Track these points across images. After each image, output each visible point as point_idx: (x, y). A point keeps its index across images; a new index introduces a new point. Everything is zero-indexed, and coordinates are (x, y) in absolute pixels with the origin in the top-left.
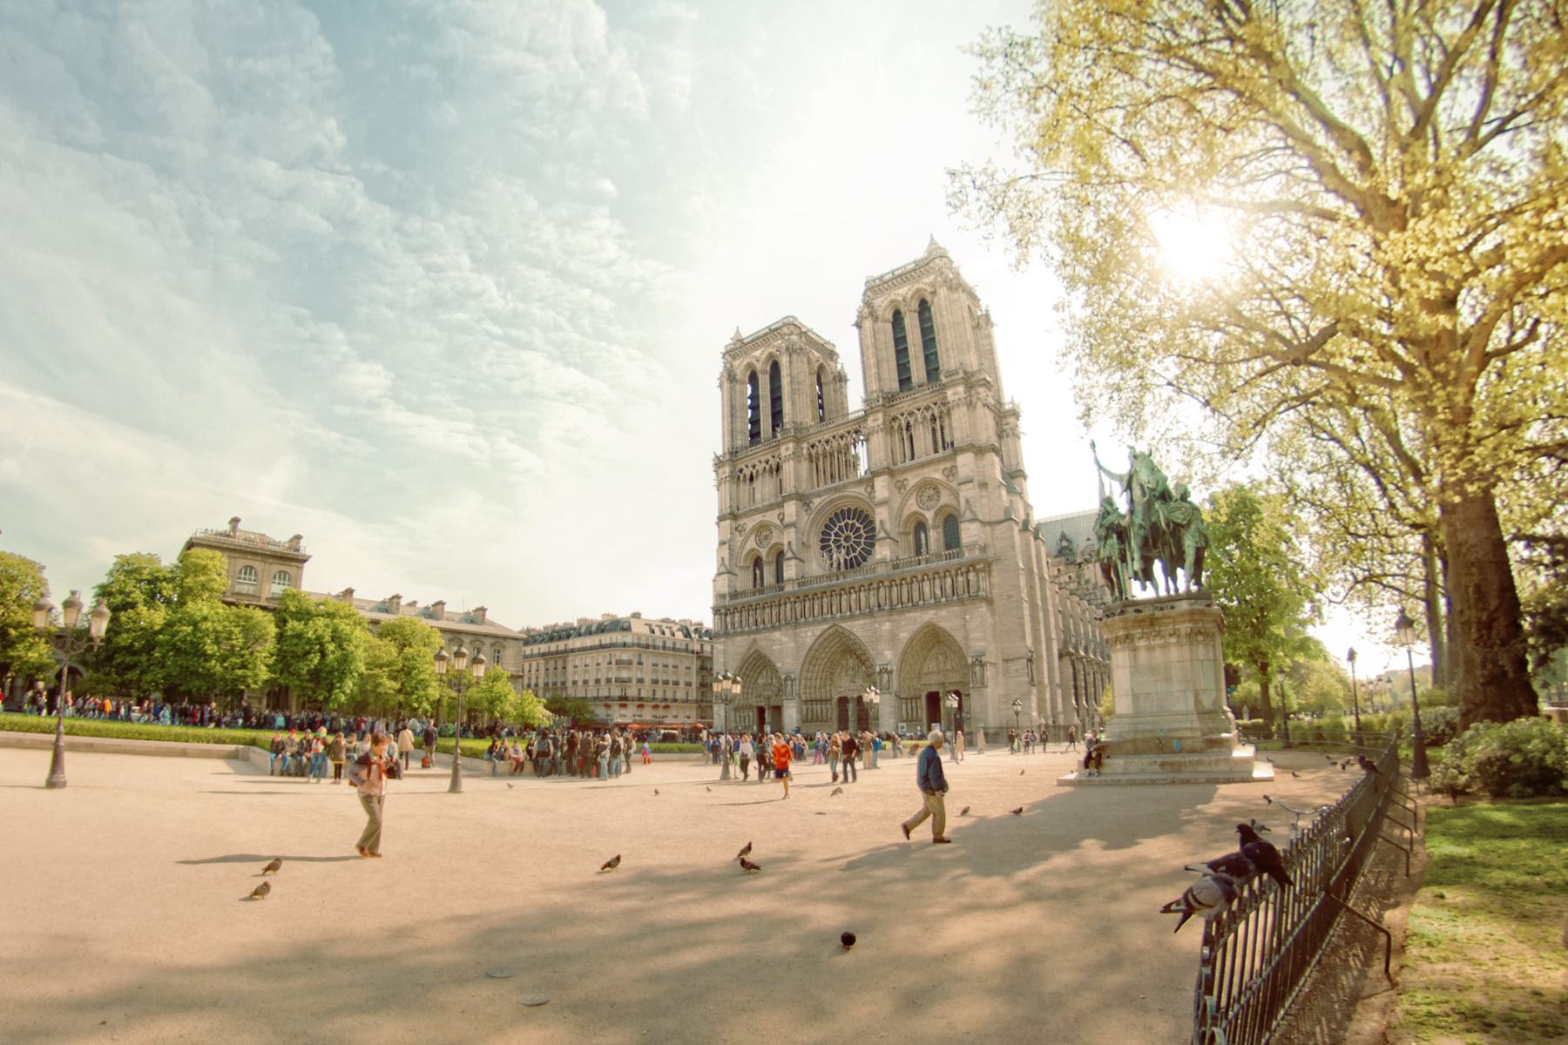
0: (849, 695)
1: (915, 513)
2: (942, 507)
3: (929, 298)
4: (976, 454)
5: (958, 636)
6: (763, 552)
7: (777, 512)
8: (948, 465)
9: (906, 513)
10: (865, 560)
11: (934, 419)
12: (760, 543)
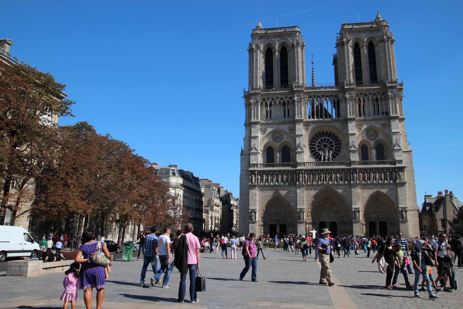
0: (326, 221)
2: (378, 140)
3: (375, 43)
5: (393, 198)
7: (287, 126)
8: (384, 122)
11: (377, 100)
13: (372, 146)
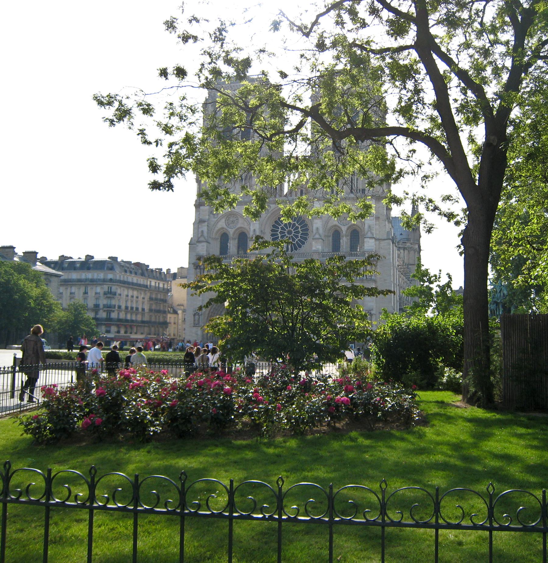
1: (335, 225)
4: (376, 200)
6: (231, 232)
9: (330, 224)
10: (300, 247)
12: (228, 224)
13: (344, 233)
